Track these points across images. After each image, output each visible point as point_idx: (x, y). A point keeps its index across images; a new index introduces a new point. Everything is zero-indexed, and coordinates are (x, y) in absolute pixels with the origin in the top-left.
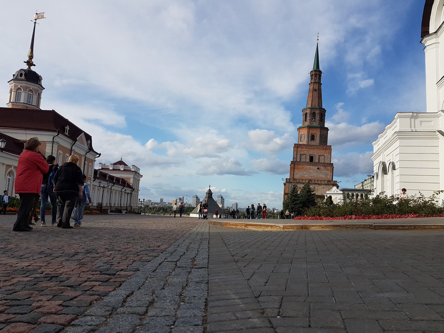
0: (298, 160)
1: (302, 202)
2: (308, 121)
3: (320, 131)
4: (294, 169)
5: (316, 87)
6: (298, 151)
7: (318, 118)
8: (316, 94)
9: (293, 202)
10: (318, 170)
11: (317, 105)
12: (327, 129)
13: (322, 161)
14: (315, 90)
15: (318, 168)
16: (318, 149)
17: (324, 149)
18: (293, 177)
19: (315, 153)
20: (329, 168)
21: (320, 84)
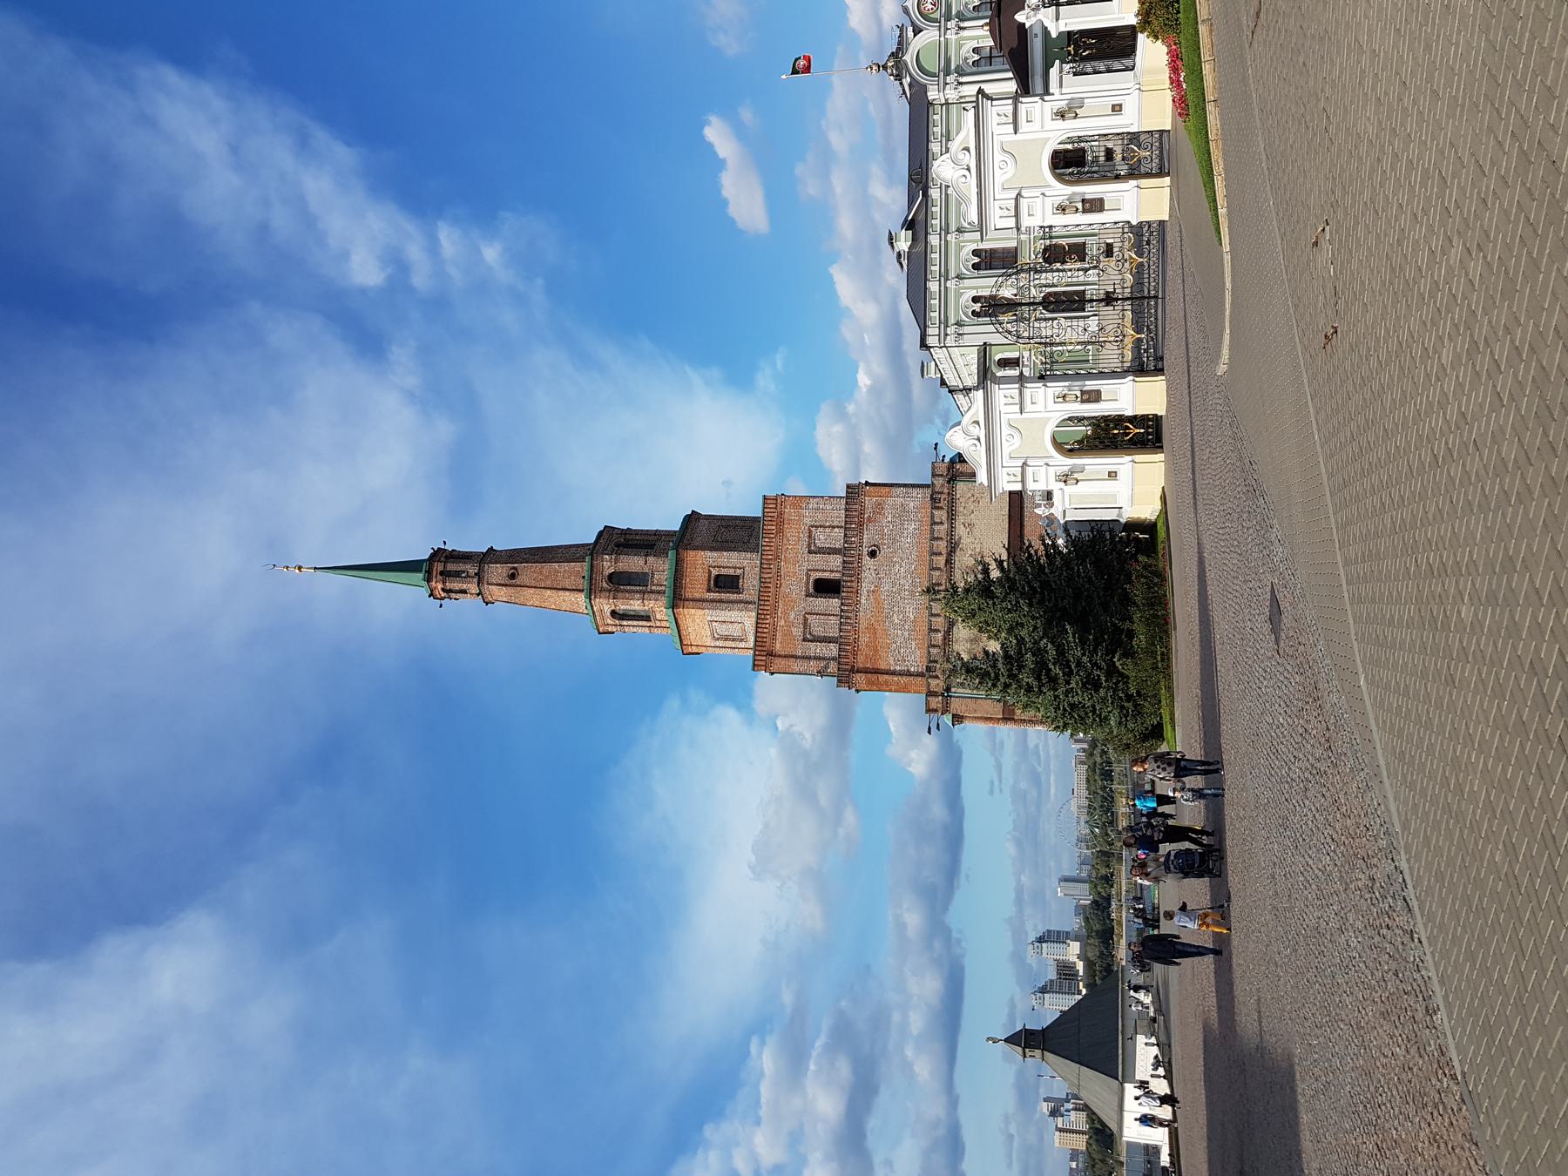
0: (832, 650)
3: (696, 548)
4: (877, 672)
5: (497, 571)
7: (633, 563)
8: (528, 572)
9: (1053, 680)
10: (879, 557)
11: (576, 566)
12: (692, 519)
13: (836, 538)
14: (513, 576)
15: (873, 554)
16: (778, 557)
17: (780, 531)
18: (921, 675)
19: (797, 569)
20: (869, 502)
21: (491, 556)
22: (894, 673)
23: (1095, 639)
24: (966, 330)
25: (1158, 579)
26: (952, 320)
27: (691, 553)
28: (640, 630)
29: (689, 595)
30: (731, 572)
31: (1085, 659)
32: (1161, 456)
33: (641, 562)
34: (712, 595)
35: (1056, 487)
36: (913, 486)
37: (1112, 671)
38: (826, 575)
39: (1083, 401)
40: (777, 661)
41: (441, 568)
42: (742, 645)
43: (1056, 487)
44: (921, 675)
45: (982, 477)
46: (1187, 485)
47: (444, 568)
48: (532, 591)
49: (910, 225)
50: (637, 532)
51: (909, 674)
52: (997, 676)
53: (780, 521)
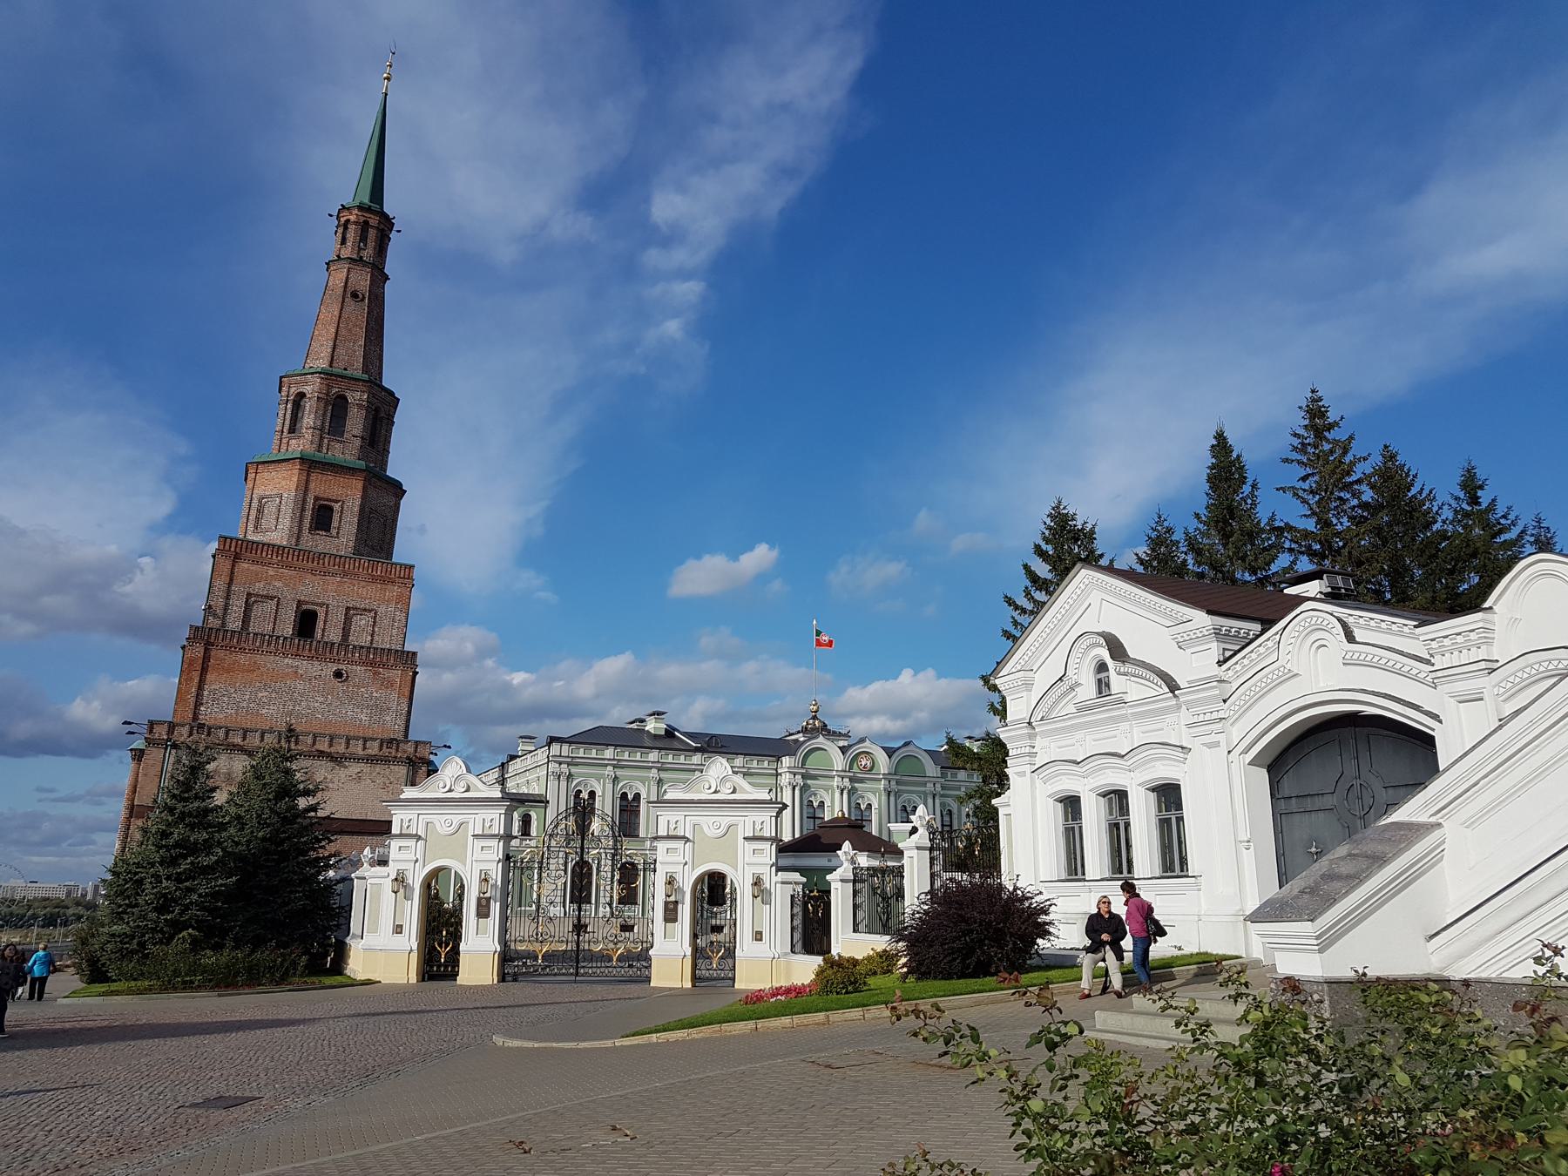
0: (234, 624)
1: (239, 858)
2: (308, 435)
3: (365, 489)
4: (204, 671)
5: (362, 280)
6: (238, 578)
7: (355, 423)
9: (173, 862)
10: (335, 682)
12: (397, 490)
13: (360, 638)
14: (355, 295)
15: (338, 674)
16: (346, 574)
17: (374, 579)
18: (195, 717)
20: (396, 674)
21: (379, 277)
22: (200, 688)
23: (217, 909)
24: (563, 784)
25: (279, 977)
26: (574, 770)
27: (360, 485)
28: (280, 421)
29: (313, 477)
30: (335, 524)
31: (195, 897)
32: (413, 979)
33: (355, 432)
34: (310, 501)
35: (392, 870)
36: (408, 721)
37: (177, 926)
38: (320, 624)
39: (479, 899)
40: (228, 564)
41: (372, 222)
42: (251, 527)
43: (392, 870)
44: (195, 717)
45: (409, 793)
46: (382, 1005)
47: (371, 226)
48: (337, 313)
49: (670, 733)
50: (389, 431)
51: (198, 704)
52: (186, 800)
53: (385, 580)
